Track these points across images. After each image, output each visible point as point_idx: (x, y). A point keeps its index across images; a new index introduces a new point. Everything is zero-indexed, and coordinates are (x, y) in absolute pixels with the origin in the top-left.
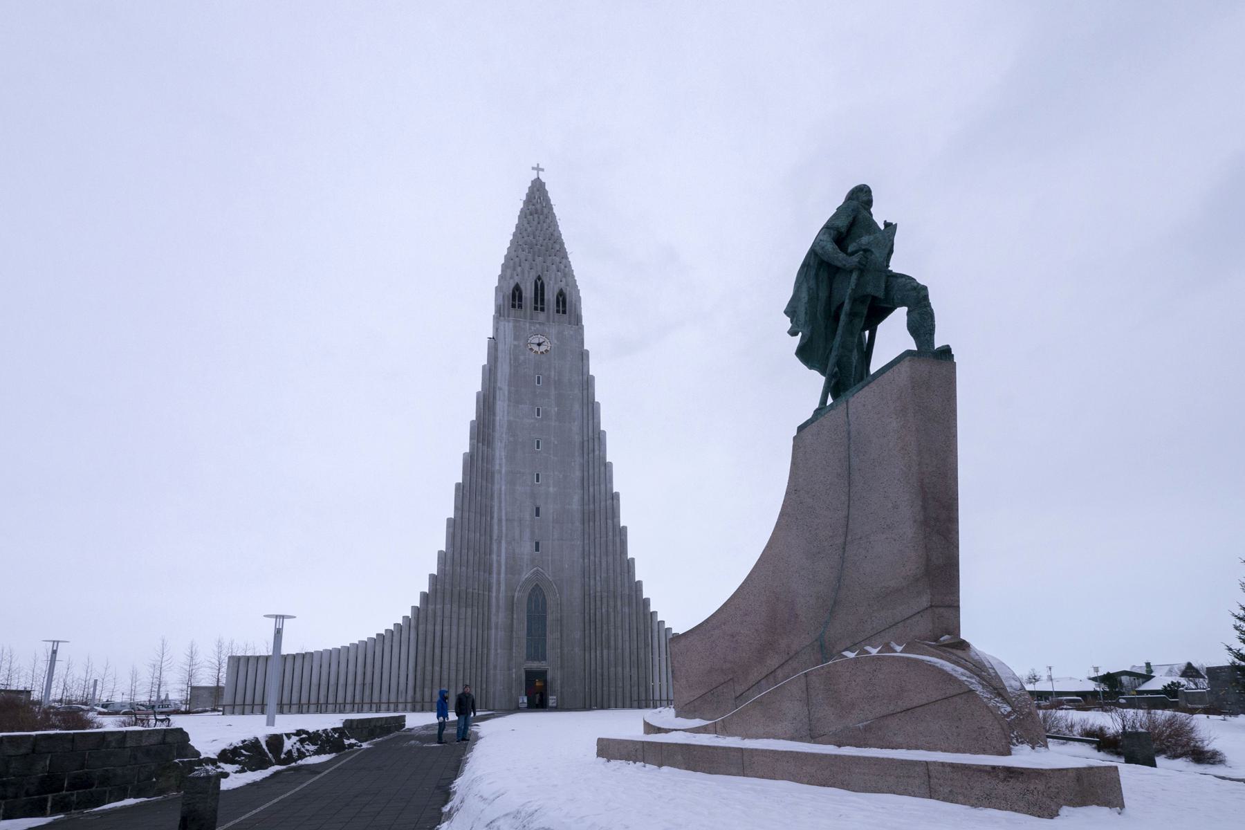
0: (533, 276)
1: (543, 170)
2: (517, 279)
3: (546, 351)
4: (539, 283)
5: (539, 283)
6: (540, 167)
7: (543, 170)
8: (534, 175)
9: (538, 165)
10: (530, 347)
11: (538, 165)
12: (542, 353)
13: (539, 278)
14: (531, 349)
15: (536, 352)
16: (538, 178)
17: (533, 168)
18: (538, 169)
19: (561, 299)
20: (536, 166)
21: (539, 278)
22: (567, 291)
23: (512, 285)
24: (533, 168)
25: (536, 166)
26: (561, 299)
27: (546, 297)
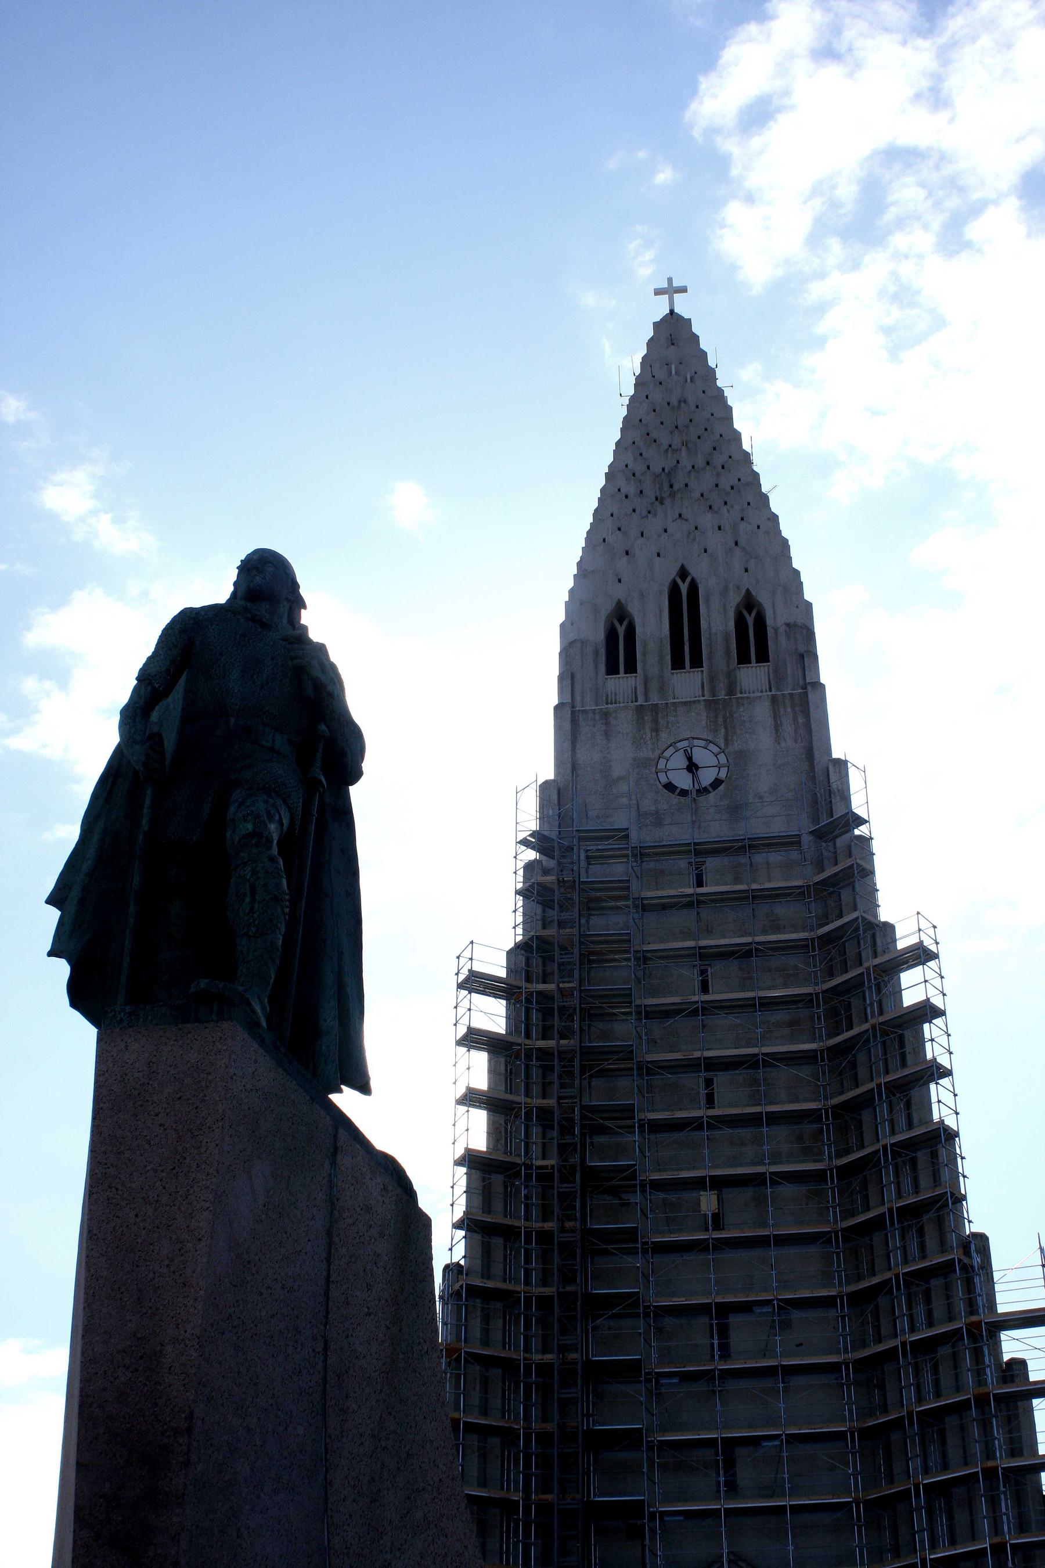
0: (665, 572)
1: (683, 290)
2: (619, 592)
3: (717, 783)
4: (684, 588)
5: (684, 588)
6: (676, 284)
7: (683, 290)
8: (660, 309)
9: (670, 280)
10: (664, 779)
11: (670, 280)
12: (703, 791)
13: (683, 573)
14: (670, 787)
15: (684, 793)
16: (672, 312)
17: (658, 292)
18: (671, 290)
19: (750, 620)
20: (666, 285)
21: (683, 573)
22: (763, 597)
23: (607, 608)
24: (658, 292)
25: (666, 285)
26: (750, 620)
27: (704, 625)
